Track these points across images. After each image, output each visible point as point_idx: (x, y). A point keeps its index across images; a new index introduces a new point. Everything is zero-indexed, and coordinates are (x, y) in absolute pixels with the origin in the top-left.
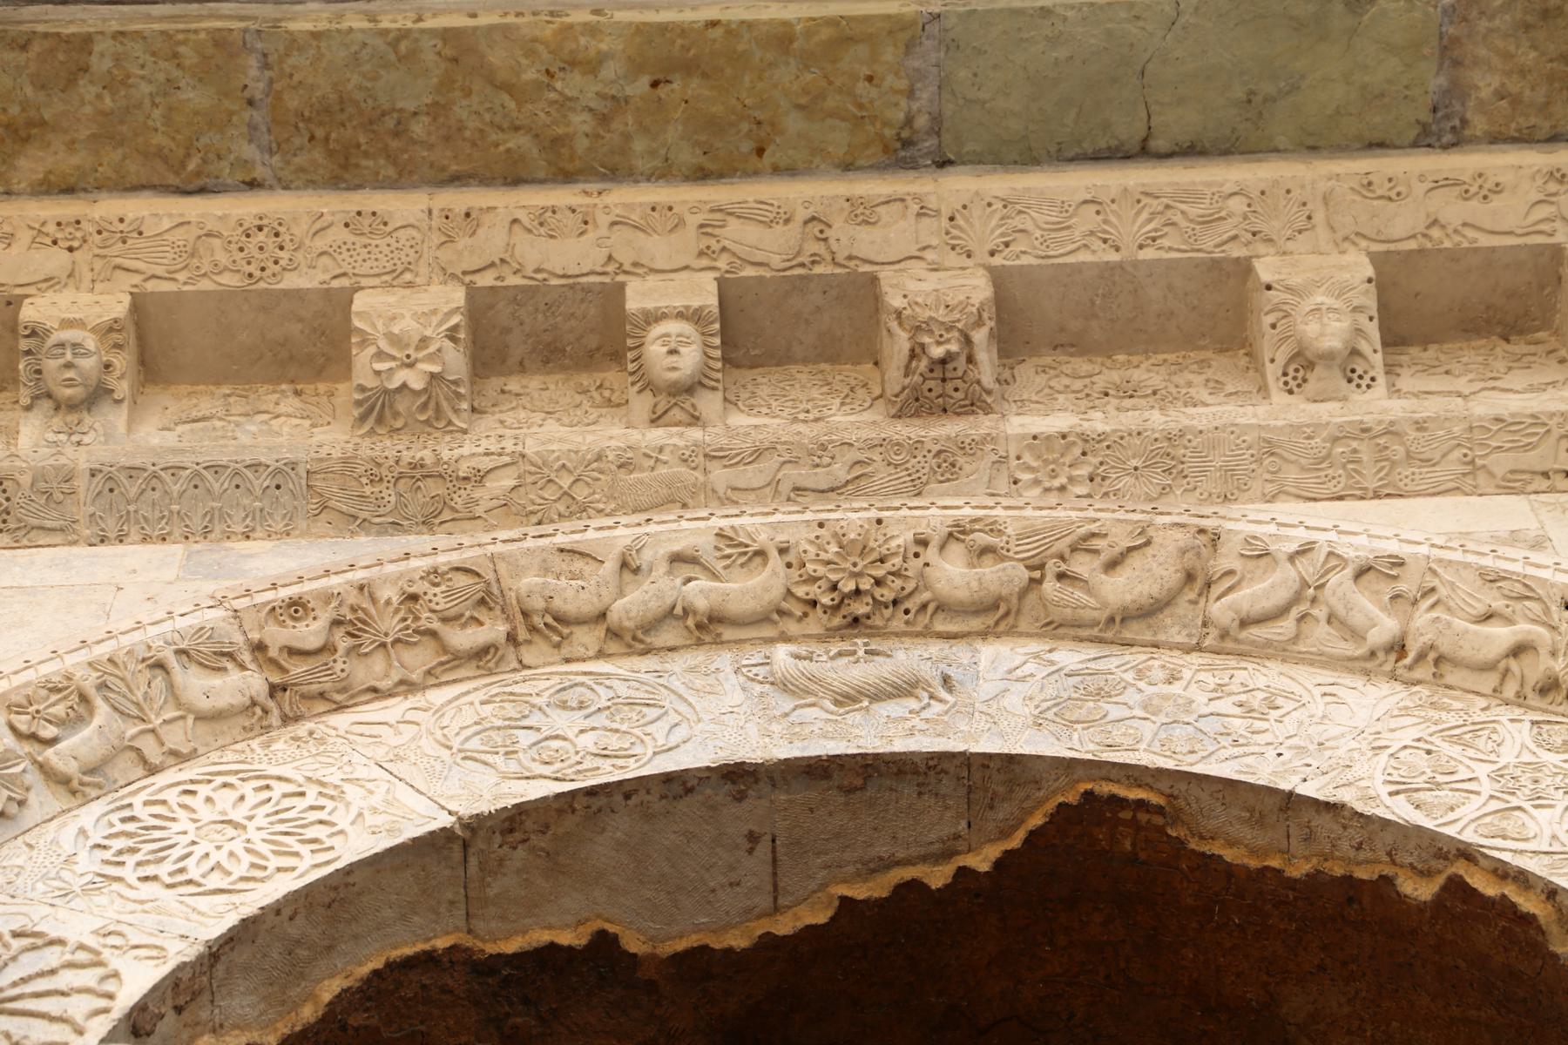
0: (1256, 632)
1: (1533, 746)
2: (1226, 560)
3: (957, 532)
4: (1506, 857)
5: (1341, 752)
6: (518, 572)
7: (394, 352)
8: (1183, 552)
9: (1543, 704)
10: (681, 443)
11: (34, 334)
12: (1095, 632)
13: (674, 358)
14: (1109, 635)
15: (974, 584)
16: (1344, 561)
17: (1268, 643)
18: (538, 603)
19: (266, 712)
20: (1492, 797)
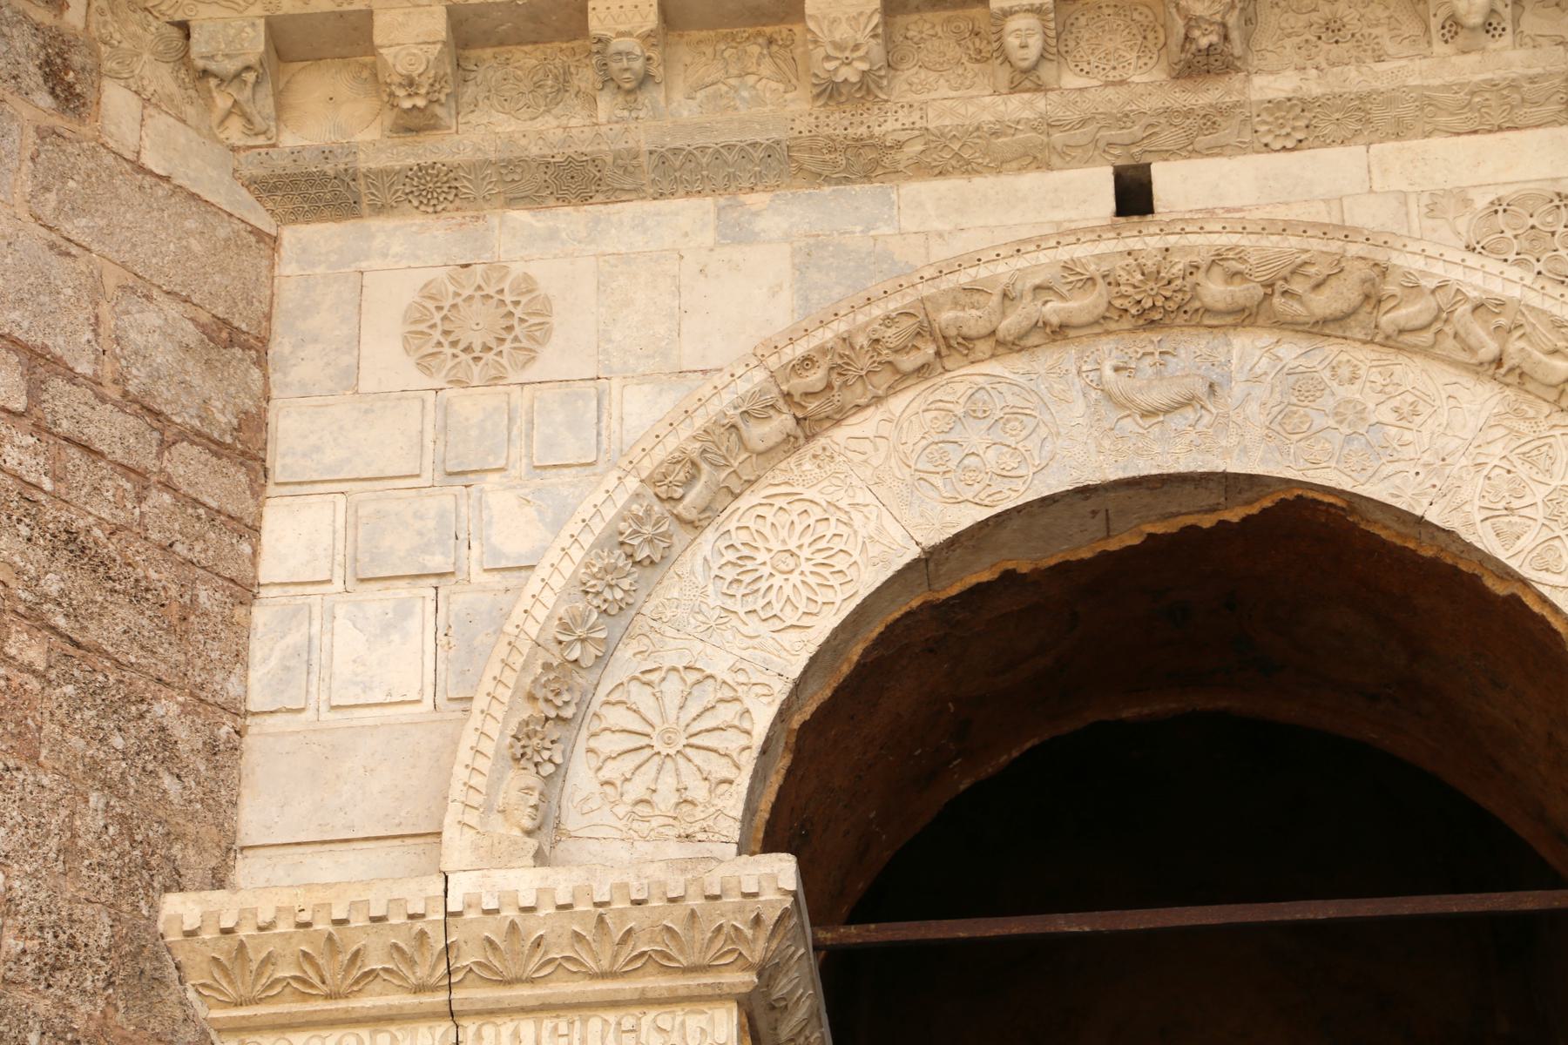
0: (1408, 338)
2: (1390, 288)
3: (1218, 259)
6: (938, 310)
7: (838, 55)
8: (1364, 281)
10: (1032, 116)
11: (600, 40)
12: (1306, 328)
13: (1025, 51)
15: (1229, 299)
16: (1467, 299)
17: (1416, 346)
18: (952, 332)
19: (796, 438)
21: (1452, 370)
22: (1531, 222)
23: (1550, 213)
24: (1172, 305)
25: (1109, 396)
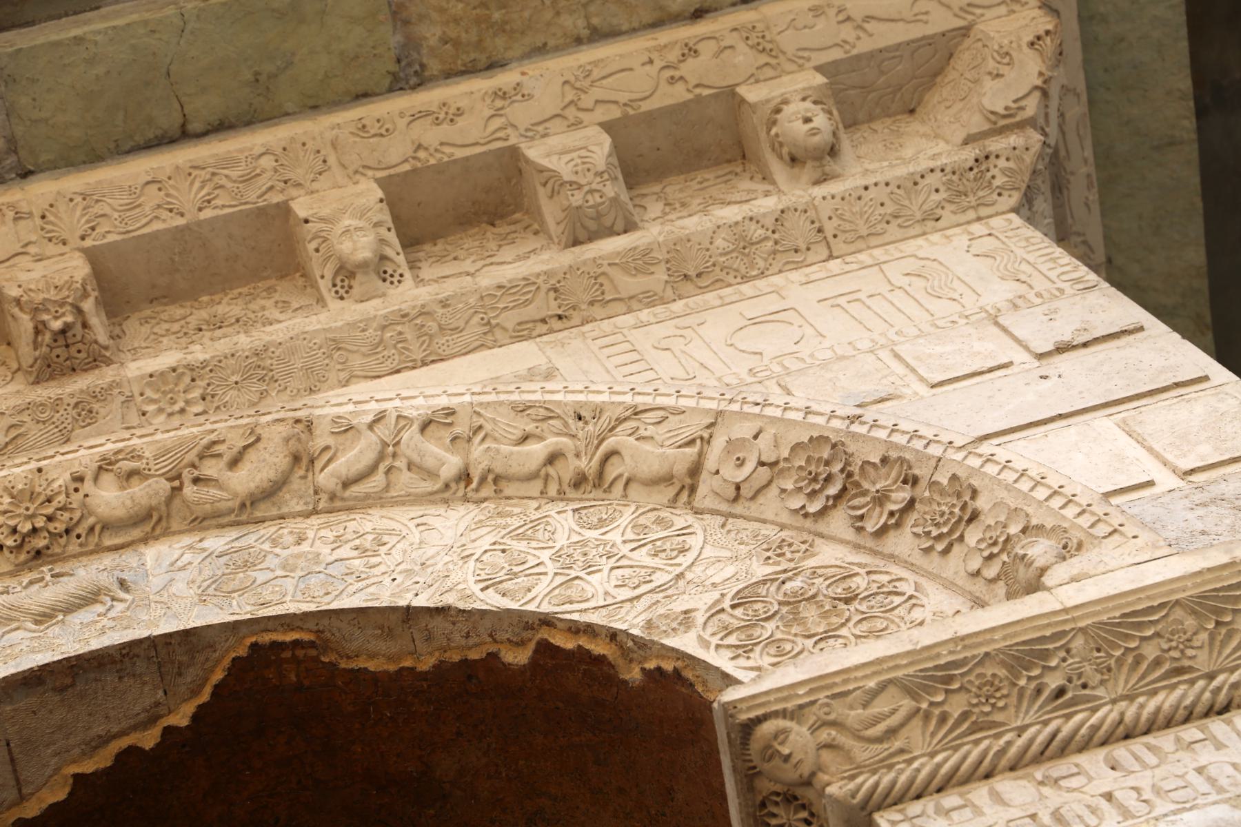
0: (356, 490)
1: (577, 528)
3: (105, 466)
4: (575, 617)
5: (439, 566)
8: (287, 440)
9: (578, 495)
12: (232, 518)
14: (244, 517)
15: (128, 503)
17: (367, 496)
20: (556, 574)
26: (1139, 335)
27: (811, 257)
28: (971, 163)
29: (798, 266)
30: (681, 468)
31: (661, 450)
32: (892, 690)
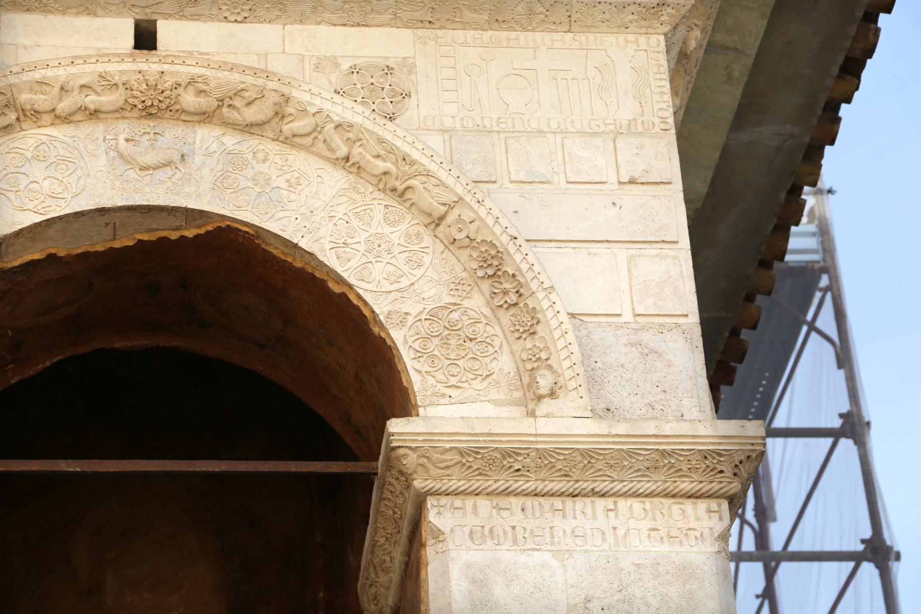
0: (297, 140)
2: (290, 110)
3: (192, 81)
6: (21, 92)
8: (275, 104)
12: (241, 128)
14: (245, 129)
15: (197, 106)
16: (332, 121)
17: (302, 145)
18: (28, 107)
21: (321, 161)
22: (372, 80)
23: (382, 77)
24: (163, 106)
25: (121, 156)
26: (668, 186)
27: (560, 28)
28: (655, 5)
29: (552, 31)
30: (436, 215)
31: (431, 200)
32: (455, 451)
